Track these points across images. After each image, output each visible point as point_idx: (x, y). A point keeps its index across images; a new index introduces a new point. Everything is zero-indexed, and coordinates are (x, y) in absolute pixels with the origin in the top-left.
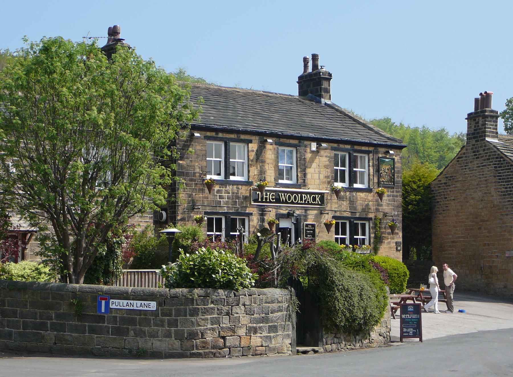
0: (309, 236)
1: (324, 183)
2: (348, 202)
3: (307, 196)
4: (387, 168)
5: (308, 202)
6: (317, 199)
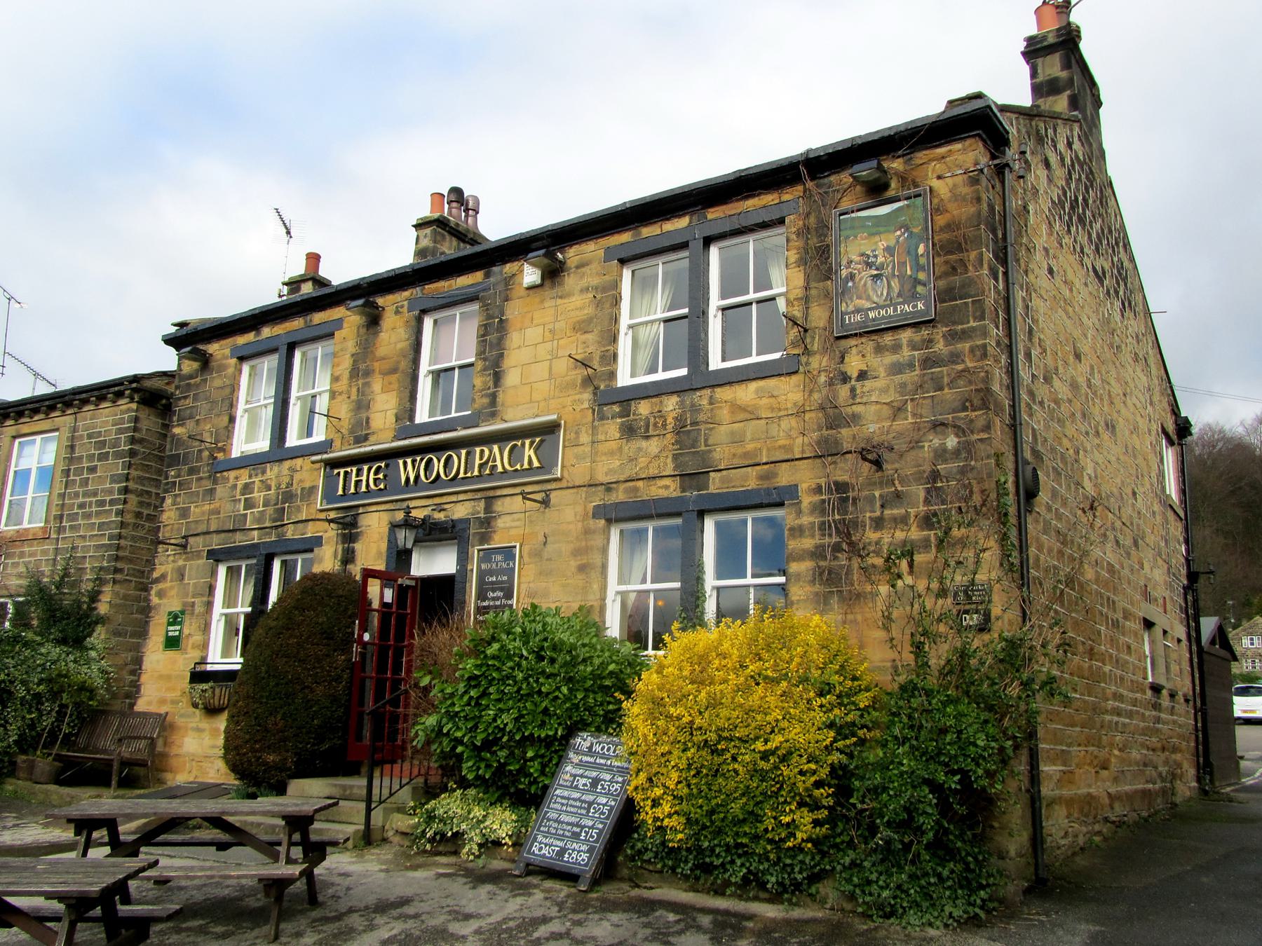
0: (491, 595)
1: (567, 387)
2: (670, 438)
3: (491, 451)
4: (882, 244)
5: (494, 467)
6: (529, 452)
